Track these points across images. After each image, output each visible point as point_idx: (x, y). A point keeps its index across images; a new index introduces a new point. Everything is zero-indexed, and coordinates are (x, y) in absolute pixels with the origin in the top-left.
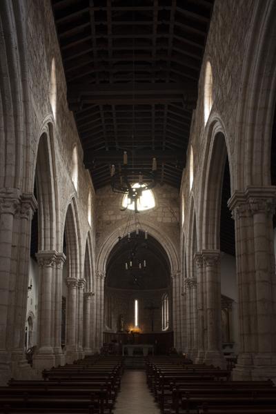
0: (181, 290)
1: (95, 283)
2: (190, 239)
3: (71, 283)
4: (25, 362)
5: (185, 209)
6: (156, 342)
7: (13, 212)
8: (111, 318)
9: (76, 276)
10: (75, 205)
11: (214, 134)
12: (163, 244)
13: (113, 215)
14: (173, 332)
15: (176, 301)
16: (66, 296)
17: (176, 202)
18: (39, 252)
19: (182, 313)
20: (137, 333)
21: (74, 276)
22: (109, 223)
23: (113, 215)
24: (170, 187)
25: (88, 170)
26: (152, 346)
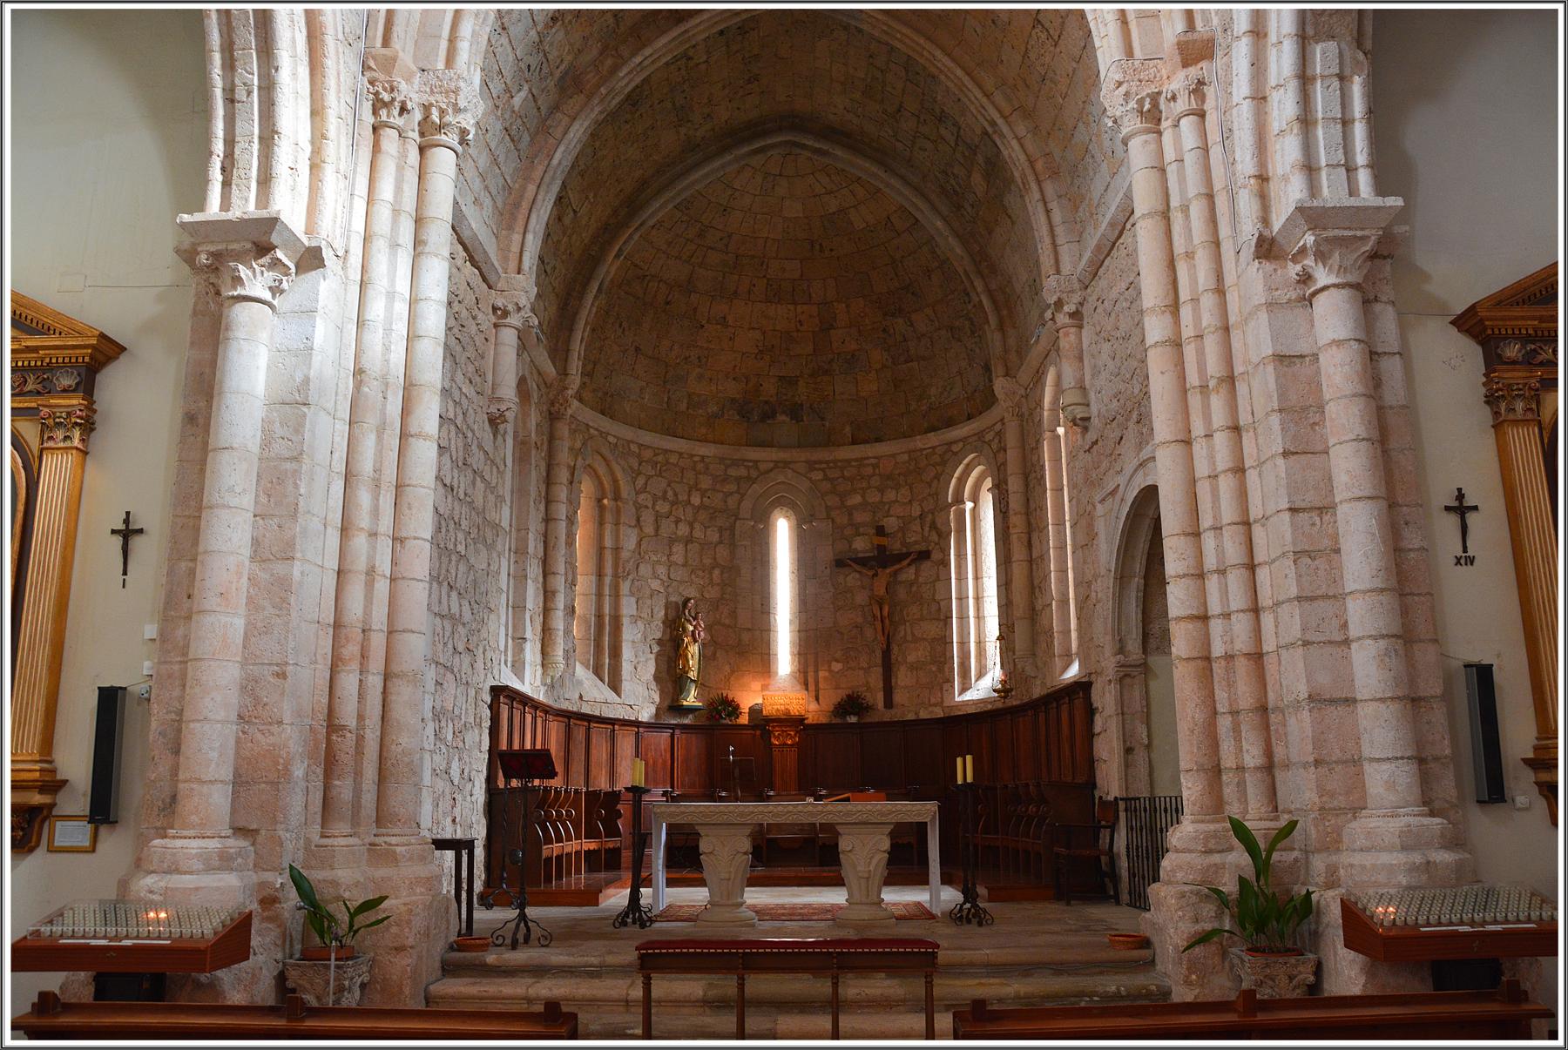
0: (1247, 205)
6: (965, 769)
19: (1270, 436)
20: (794, 722)
26: (925, 811)
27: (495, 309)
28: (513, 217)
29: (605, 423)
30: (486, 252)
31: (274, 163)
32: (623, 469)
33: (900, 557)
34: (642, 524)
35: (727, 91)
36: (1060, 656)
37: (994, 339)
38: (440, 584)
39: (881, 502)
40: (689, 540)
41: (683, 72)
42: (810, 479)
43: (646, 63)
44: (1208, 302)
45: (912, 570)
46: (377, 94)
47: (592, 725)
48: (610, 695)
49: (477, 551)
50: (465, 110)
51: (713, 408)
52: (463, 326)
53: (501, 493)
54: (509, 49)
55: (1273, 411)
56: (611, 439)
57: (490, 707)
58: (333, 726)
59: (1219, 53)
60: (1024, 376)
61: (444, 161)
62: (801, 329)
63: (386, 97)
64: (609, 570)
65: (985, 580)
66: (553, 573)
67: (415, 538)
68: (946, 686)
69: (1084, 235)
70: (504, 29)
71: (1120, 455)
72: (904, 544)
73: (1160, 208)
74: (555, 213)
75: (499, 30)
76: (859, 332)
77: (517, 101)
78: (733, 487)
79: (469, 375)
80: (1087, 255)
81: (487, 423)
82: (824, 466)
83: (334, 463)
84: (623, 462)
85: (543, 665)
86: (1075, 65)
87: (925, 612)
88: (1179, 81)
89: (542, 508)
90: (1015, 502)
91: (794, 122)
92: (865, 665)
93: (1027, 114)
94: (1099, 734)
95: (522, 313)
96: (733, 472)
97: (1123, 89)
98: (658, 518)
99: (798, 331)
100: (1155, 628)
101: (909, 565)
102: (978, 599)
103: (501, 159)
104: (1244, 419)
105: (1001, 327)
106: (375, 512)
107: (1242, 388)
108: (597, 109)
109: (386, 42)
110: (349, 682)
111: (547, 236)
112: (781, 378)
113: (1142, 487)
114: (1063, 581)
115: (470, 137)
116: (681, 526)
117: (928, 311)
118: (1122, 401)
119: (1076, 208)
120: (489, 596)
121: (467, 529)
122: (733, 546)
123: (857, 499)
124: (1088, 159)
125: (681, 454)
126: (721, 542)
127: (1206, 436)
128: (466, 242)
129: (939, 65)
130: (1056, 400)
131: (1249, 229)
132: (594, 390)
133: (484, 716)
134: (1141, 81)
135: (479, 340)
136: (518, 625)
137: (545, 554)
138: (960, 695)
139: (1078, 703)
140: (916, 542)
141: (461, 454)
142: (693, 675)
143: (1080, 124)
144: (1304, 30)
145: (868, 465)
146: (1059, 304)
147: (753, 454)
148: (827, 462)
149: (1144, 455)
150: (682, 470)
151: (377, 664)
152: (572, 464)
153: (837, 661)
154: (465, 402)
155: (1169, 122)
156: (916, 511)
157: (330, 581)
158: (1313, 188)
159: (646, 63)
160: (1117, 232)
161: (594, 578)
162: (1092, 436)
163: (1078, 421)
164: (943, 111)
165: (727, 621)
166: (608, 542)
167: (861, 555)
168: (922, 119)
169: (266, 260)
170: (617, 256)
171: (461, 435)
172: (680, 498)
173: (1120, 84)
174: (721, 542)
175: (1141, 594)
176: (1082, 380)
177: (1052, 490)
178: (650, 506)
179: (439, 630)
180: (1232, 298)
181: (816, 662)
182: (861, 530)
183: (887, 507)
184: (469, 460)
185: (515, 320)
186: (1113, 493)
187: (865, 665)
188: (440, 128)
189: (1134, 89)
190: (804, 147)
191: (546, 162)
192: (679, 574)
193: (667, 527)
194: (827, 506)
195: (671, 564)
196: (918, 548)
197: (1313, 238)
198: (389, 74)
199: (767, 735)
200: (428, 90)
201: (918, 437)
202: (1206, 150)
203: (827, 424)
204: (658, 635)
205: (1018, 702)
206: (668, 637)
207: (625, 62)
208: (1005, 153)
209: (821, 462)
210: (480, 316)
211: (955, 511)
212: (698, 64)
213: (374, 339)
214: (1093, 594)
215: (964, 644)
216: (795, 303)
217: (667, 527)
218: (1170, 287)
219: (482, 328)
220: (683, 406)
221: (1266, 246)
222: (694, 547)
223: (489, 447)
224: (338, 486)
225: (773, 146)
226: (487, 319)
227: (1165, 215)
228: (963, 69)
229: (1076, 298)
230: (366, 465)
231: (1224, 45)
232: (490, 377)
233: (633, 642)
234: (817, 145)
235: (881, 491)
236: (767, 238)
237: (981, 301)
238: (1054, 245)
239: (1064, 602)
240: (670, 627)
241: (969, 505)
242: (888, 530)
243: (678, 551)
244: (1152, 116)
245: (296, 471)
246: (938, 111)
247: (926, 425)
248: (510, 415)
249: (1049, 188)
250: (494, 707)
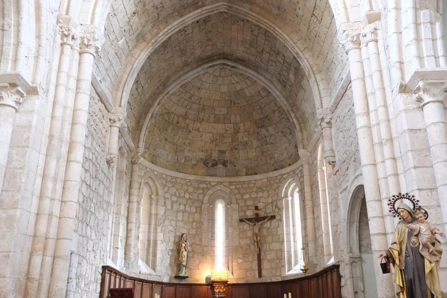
0: (396, 73)
8: (155, 242)
20: (225, 283)
27: (110, 120)
28: (118, 86)
29: (153, 166)
30: (107, 98)
31: (19, 54)
32: (160, 184)
33: (264, 218)
34: (166, 205)
35: (199, 44)
36: (326, 255)
37: (299, 135)
38: (83, 223)
39: (257, 197)
40: (184, 211)
41: (183, 36)
42: (230, 189)
43: (169, 31)
44: (381, 110)
45: (269, 223)
46: (63, 32)
47: (144, 283)
48: (152, 272)
49: (99, 212)
50: (98, 40)
51: (194, 162)
52: (97, 125)
53: (110, 190)
54: (117, 23)
55: (409, 151)
56: (156, 173)
57: (102, 275)
58: (28, 278)
59: (382, 18)
60: (310, 148)
61: (88, 59)
62: (227, 133)
63: (66, 33)
64: (153, 222)
65: (296, 227)
66: (131, 223)
67: (71, 201)
68: (282, 269)
69: (332, 93)
70: (115, 15)
71: (347, 174)
72: (265, 213)
73: (361, 76)
74: (135, 86)
75: (113, 15)
76: (248, 134)
77: (120, 43)
78: (201, 191)
79: (99, 144)
80: (333, 100)
81: (105, 162)
82: (235, 184)
83: (38, 171)
84: (159, 181)
85: (125, 259)
86: (327, 30)
87: (274, 240)
88: (368, 28)
89: (127, 197)
90: (308, 196)
91: (225, 56)
92: (251, 260)
93: (311, 49)
94: (343, 286)
95: (121, 122)
96: (201, 186)
97: (346, 33)
98: (172, 202)
99: (226, 133)
100: (364, 243)
101: (268, 221)
102: (294, 234)
103: (114, 64)
104: (397, 155)
105: (301, 131)
106: (54, 191)
107: (396, 143)
108: (151, 48)
109: (67, 13)
110: (37, 260)
111: (132, 95)
112: (219, 151)
113: (357, 185)
114: (327, 226)
115: (99, 50)
116: (181, 206)
117: (274, 126)
118: (348, 154)
119: (329, 84)
120: (104, 230)
121: (96, 203)
122: (201, 213)
123: (247, 196)
124: (333, 65)
125: (182, 179)
126: (196, 212)
127: (382, 162)
128: (99, 93)
129: (277, 33)
130: (322, 156)
131: (397, 82)
132: (149, 154)
133: (99, 278)
134: (352, 30)
135: (104, 131)
136: (115, 242)
137: (128, 215)
138: (288, 272)
139: (335, 274)
140: (270, 212)
141: (94, 173)
142: (184, 263)
143: (330, 52)
144: (415, 6)
145: (252, 183)
146: (322, 119)
147: (209, 179)
148: (237, 182)
149: (358, 173)
150: (182, 185)
151: (50, 252)
152: (140, 181)
153: (240, 258)
154: (96, 153)
155: (364, 45)
156: (270, 200)
157: (33, 218)
158: (422, 65)
159: (169, 31)
160: (344, 91)
161: (147, 226)
162: (336, 168)
163: (331, 163)
164: (279, 51)
165: (198, 243)
166: (153, 212)
167: (249, 217)
168: (271, 54)
169: (14, 90)
170: (159, 104)
171: (94, 166)
172: (181, 195)
173: (345, 31)
174: (196, 212)
175: (358, 229)
176: (332, 147)
177: (322, 191)
178: (170, 198)
179: (81, 241)
180: (391, 109)
181: (232, 259)
182: (250, 208)
183: (259, 199)
184: (97, 176)
185: (118, 124)
186: (345, 190)
187: (251, 260)
188: (87, 46)
189: (350, 33)
190: (228, 65)
191: (131, 67)
192: (181, 224)
193: (176, 206)
194: (236, 199)
195: (177, 221)
196: (271, 214)
197: (422, 83)
198: (68, 25)
199: (213, 288)
200: (83, 32)
201: (271, 173)
202: (378, 54)
203: (237, 168)
204: (171, 248)
205: (311, 275)
206: (175, 249)
207: (161, 31)
208: (302, 64)
209: (234, 182)
210: (104, 122)
211: (285, 200)
212: (189, 34)
213: (57, 124)
214: (339, 230)
215: (289, 252)
216: (224, 123)
217: (176, 206)
218: (366, 106)
219: (105, 126)
220: (183, 161)
221: (403, 88)
222: (186, 214)
223: (106, 172)
224: (39, 180)
225: (216, 65)
226: (106, 123)
228: (286, 34)
229: (329, 117)
230: (52, 172)
231: (384, 15)
232: (107, 146)
233: (161, 250)
234: (233, 65)
235: (257, 192)
236: (215, 99)
237: (293, 121)
238: (321, 97)
239: (328, 234)
240: (176, 245)
241: (290, 198)
242: (259, 208)
243: (180, 215)
244: (357, 43)
245: (21, 173)
246: (277, 51)
247: (273, 168)
248: (115, 160)
249: (318, 76)
250: (103, 275)
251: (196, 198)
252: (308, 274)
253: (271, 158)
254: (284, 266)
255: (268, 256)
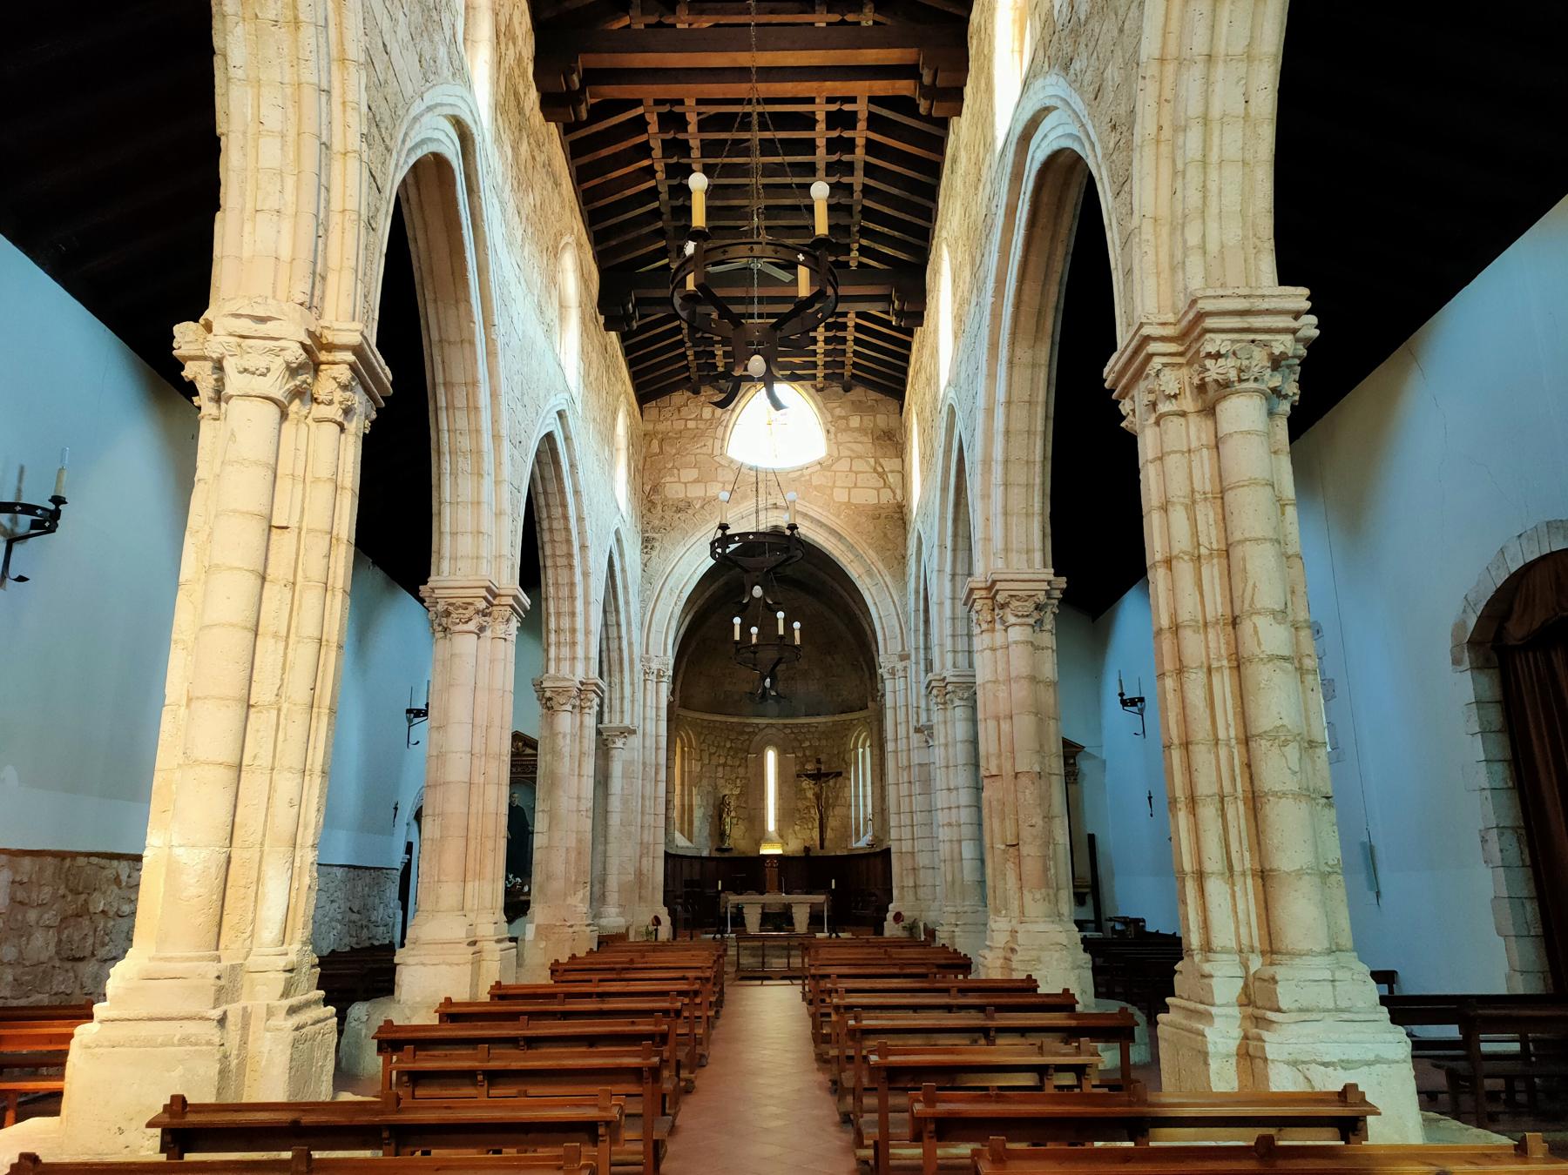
1: (639, 695)
2: (942, 546)
3: (558, 691)
4: (307, 1005)
5: (923, 457)
7: (279, 394)
8: (691, 806)
9: (573, 672)
10: (567, 438)
11: (1039, 152)
12: (854, 571)
13: (696, 481)
14: (888, 851)
15: (896, 752)
16: (531, 731)
17: (892, 441)
18: (433, 580)
21: (565, 666)
22: (683, 507)
23: (696, 481)
24: (874, 395)
25: (613, 334)
26: (820, 898)
33: (827, 775)
40: (724, 765)
44: (904, 741)
48: (688, 844)
58: (641, 873)
98: (710, 754)
109: (647, 652)
142: (728, 832)
151: (651, 855)
213: (647, 753)
215: (857, 819)
217: (714, 762)
227: (895, 709)
230: (647, 794)
241: (861, 750)
243: (720, 769)
251: (740, 746)
252: (873, 850)
253: (839, 696)
254: (851, 837)
255: (832, 823)
